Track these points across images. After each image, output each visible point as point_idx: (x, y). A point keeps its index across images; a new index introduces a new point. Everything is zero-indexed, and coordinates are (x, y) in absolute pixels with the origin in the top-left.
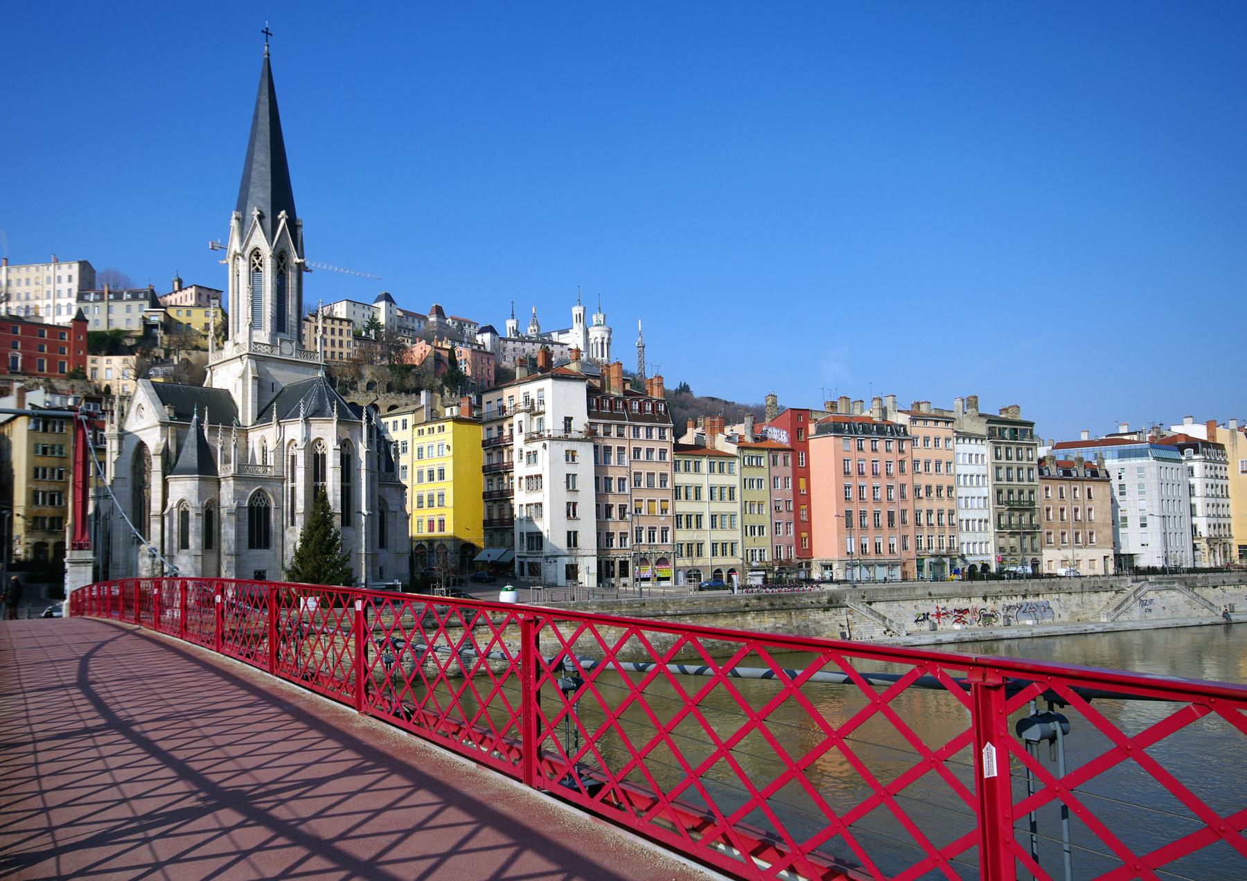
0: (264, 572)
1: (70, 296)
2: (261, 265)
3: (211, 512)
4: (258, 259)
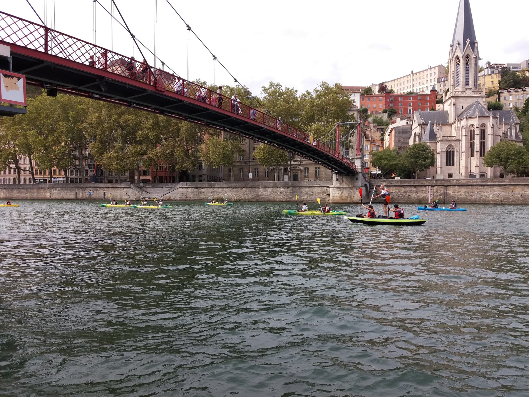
0: (452, 174)
2: (459, 62)
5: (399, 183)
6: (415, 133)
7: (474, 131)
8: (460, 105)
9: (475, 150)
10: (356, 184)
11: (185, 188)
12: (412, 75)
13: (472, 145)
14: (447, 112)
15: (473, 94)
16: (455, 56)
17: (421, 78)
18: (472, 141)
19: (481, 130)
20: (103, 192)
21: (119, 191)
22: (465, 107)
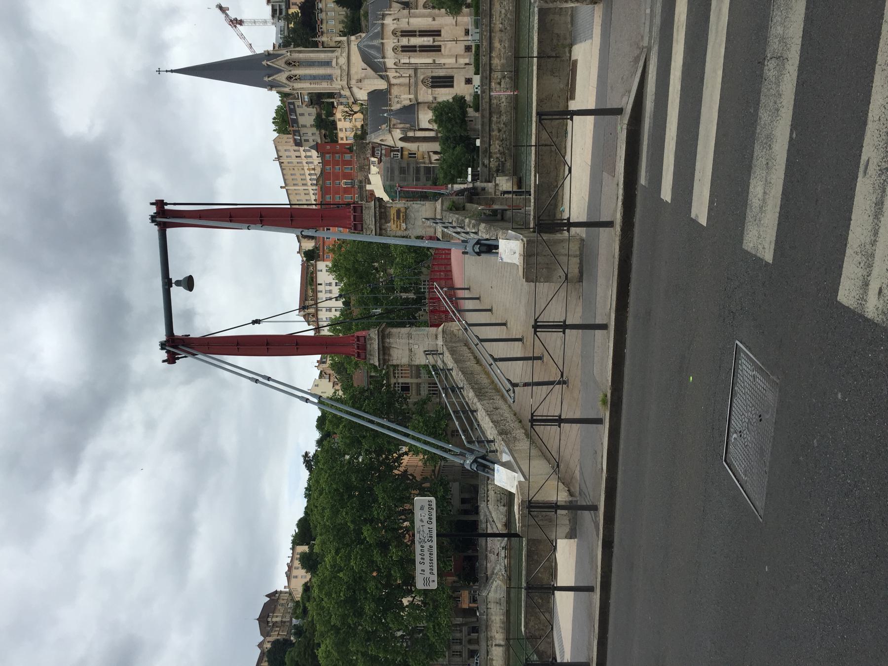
0: (466, 79)
1: (299, 151)
2: (296, 76)
3: (432, 77)
4: (292, 78)
5: (485, 139)
6: (401, 139)
7: (402, 47)
8: (362, 74)
9: (431, 43)
10: (490, 190)
11: (488, 497)
12: (286, 188)
13: (424, 49)
14: (370, 94)
15: (345, 54)
16: (287, 82)
17: (293, 172)
18: (418, 49)
19: (402, 36)
20: (494, 648)
21: (493, 618)
22: (365, 66)
